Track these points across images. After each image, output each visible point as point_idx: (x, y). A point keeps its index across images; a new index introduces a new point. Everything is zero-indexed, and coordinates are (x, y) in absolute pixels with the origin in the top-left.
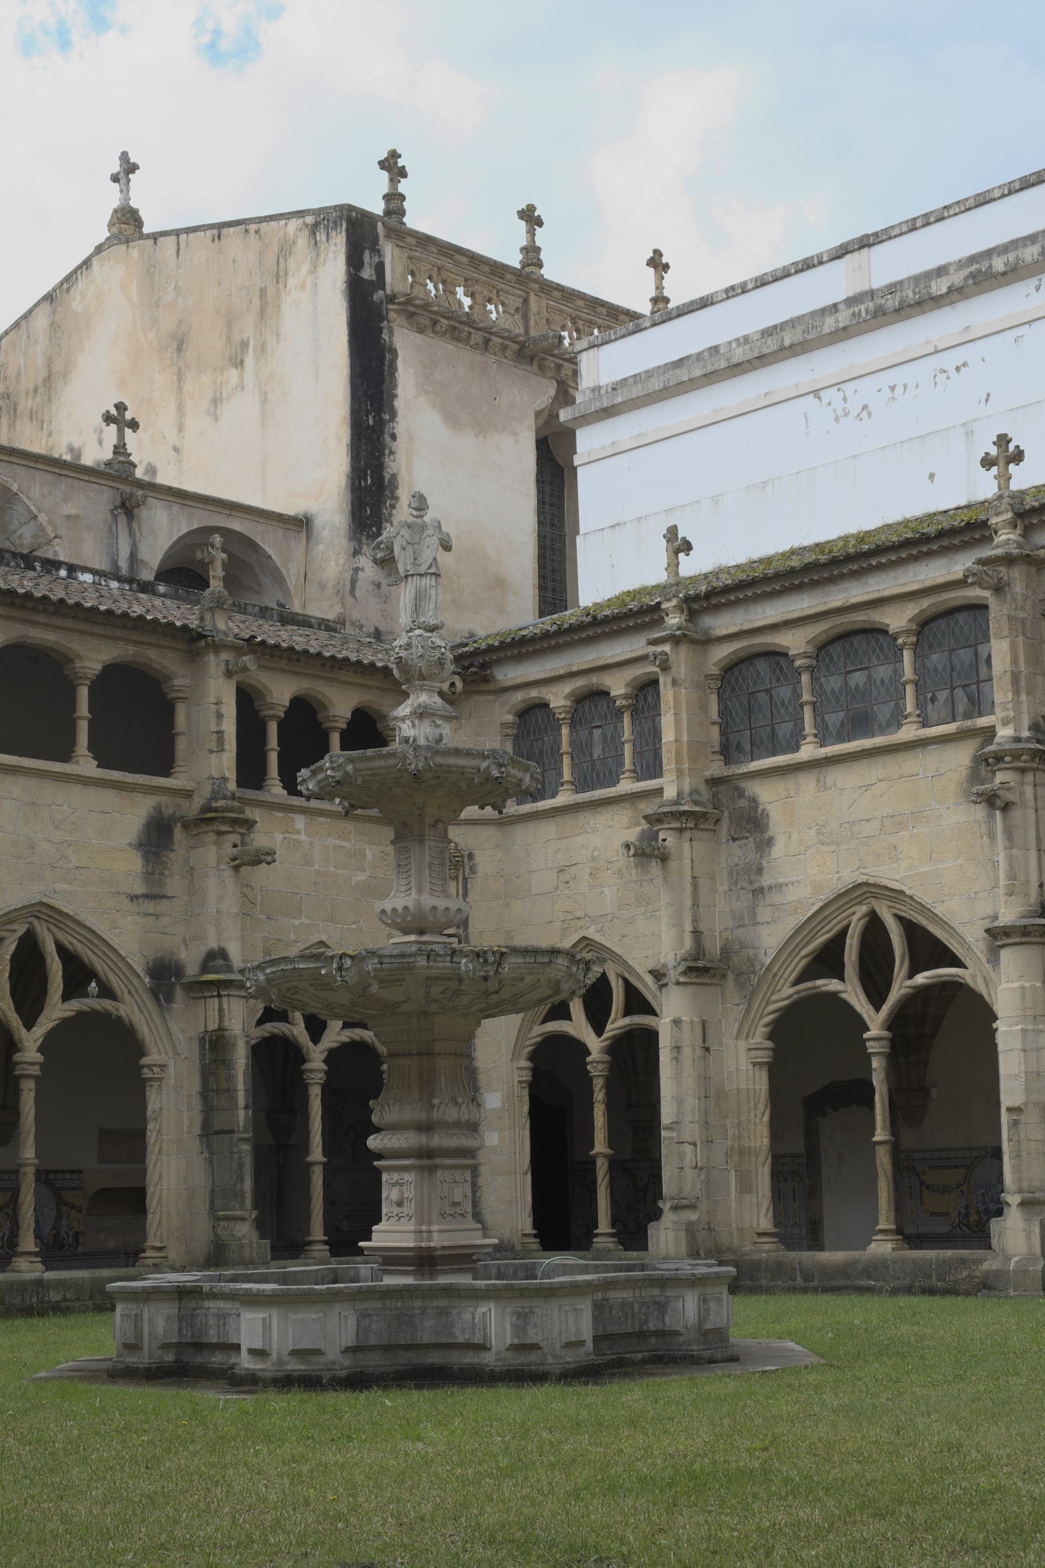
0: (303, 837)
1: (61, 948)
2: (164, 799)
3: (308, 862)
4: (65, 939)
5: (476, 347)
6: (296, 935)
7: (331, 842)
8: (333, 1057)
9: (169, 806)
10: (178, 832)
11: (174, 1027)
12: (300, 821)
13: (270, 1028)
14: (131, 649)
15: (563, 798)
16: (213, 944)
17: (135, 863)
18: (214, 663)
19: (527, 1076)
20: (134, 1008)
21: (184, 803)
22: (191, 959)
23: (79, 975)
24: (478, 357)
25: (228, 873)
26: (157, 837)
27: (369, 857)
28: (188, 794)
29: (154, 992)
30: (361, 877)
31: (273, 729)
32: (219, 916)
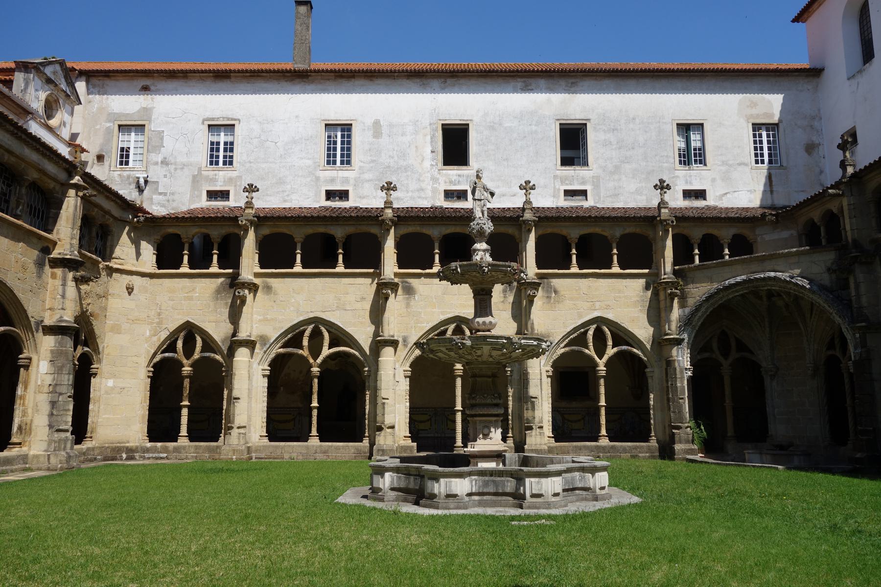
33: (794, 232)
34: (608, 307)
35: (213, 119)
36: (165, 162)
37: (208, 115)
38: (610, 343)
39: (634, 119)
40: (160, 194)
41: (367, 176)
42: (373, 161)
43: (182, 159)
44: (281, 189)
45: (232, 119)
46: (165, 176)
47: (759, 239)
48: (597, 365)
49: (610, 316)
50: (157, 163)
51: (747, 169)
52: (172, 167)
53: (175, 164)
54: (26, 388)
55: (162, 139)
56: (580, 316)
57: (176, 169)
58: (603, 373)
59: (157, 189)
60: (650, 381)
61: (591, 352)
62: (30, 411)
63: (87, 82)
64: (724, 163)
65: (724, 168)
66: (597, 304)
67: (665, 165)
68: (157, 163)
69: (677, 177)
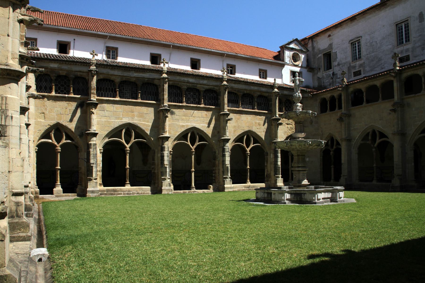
35: (352, 40)
36: (339, 65)
37: (350, 39)
40: (338, 78)
41: (417, 45)
42: (420, 35)
43: (344, 61)
44: (380, 63)
45: (358, 38)
46: (339, 70)
50: (336, 66)
52: (341, 66)
53: (342, 64)
54: (267, 163)
55: (336, 55)
57: (342, 66)
59: (337, 76)
62: (269, 170)
63: (312, 41)
68: (336, 66)
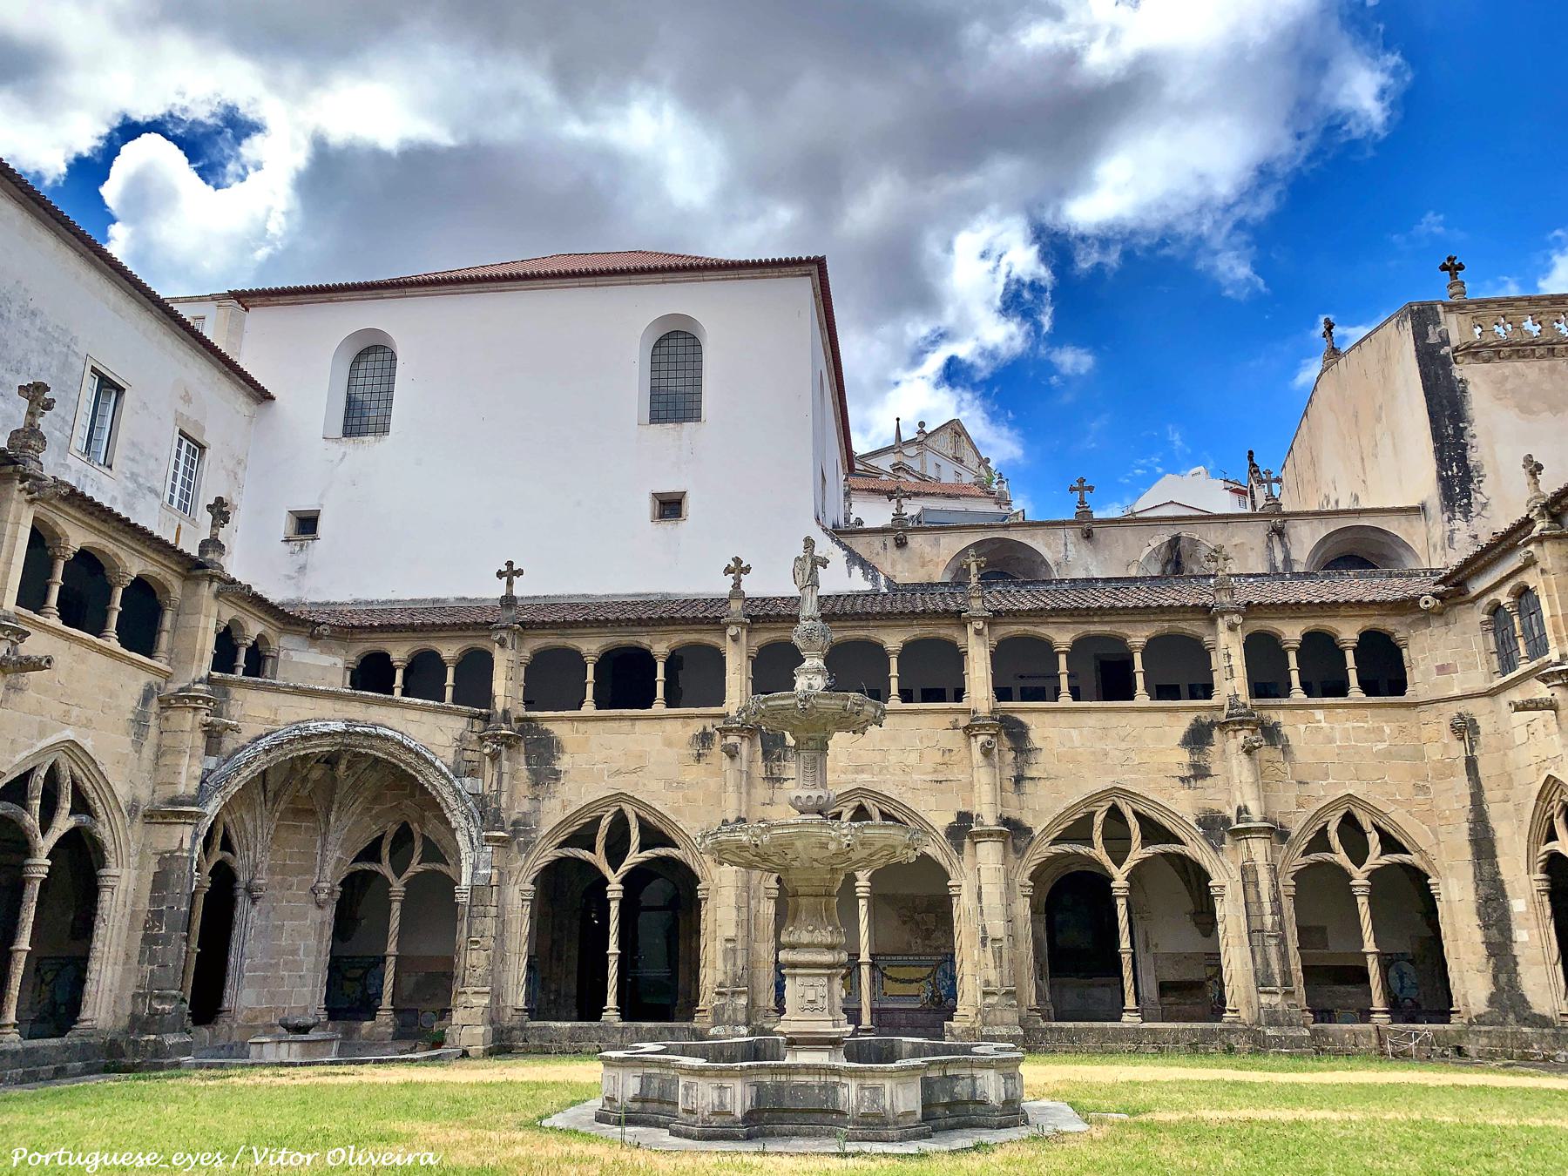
0: (1323, 724)
1: (1136, 813)
2: (1202, 714)
3: (1331, 741)
4: (1140, 809)
5: (1542, 357)
6: (1327, 791)
7: (1349, 725)
8: (1374, 875)
9: (1206, 717)
10: (1216, 733)
11: (1225, 860)
12: (1319, 714)
13: (1314, 857)
14: (1166, 625)
15: (1523, 667)
16: (1239, 802)
17: (1185, 756)
18: (1222, 624)
19: (1545, 886)
20: (1196, 849)
21: (1218, 714)
22: (1231, 813)
23: (1154, 831)
24: (1546, 363)
25: (1243, 757)
26: (1198, 738)
27: (1388, 731)
28: (1221, 708)
29: (1206, 837)
30: (1381, 746)
31: (1292, 657)
32: (1236, 782)
33: (340, 663)
34: (88, 724)
38: (66, 805)
39: (34, 314)
47: (282, 655)
48: (25, 848)
49: (88, 745)
51: (157, 503)
56: (42, 734)
58: (42, 872)
60: (105, 896)
61: (32, 820)
64: (134, 477)
65: (131, 486)
66: (75, 711)
67: (57, 433)
69: (68, 467)
